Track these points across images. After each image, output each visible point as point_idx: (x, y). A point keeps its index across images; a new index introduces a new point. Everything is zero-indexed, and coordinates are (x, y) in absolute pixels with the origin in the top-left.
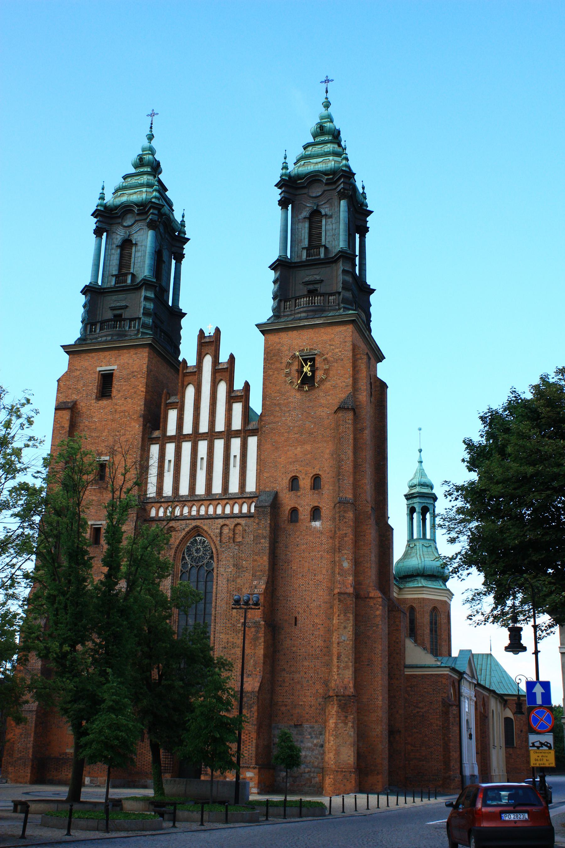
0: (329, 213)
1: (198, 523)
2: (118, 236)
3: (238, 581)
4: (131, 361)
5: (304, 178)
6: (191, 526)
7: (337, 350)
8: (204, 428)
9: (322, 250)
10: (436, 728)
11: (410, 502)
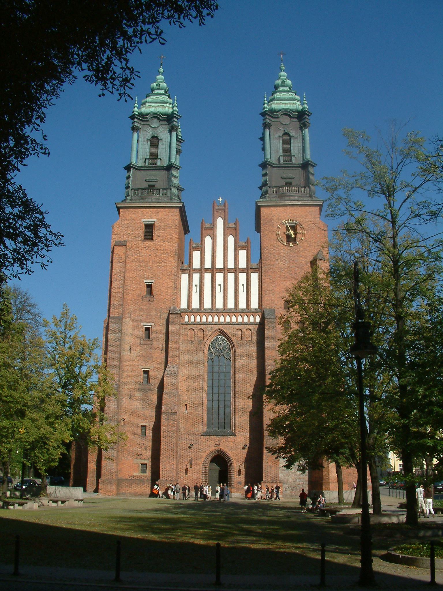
0: (296, 136)
1: (220, 327)
2: (148, 133)
3: (250, 365)
4: (166, 217)
5: (278, 112)
6: (214, 329)
7: (310, 223)
8: (219, 265)
9: (293, 158)
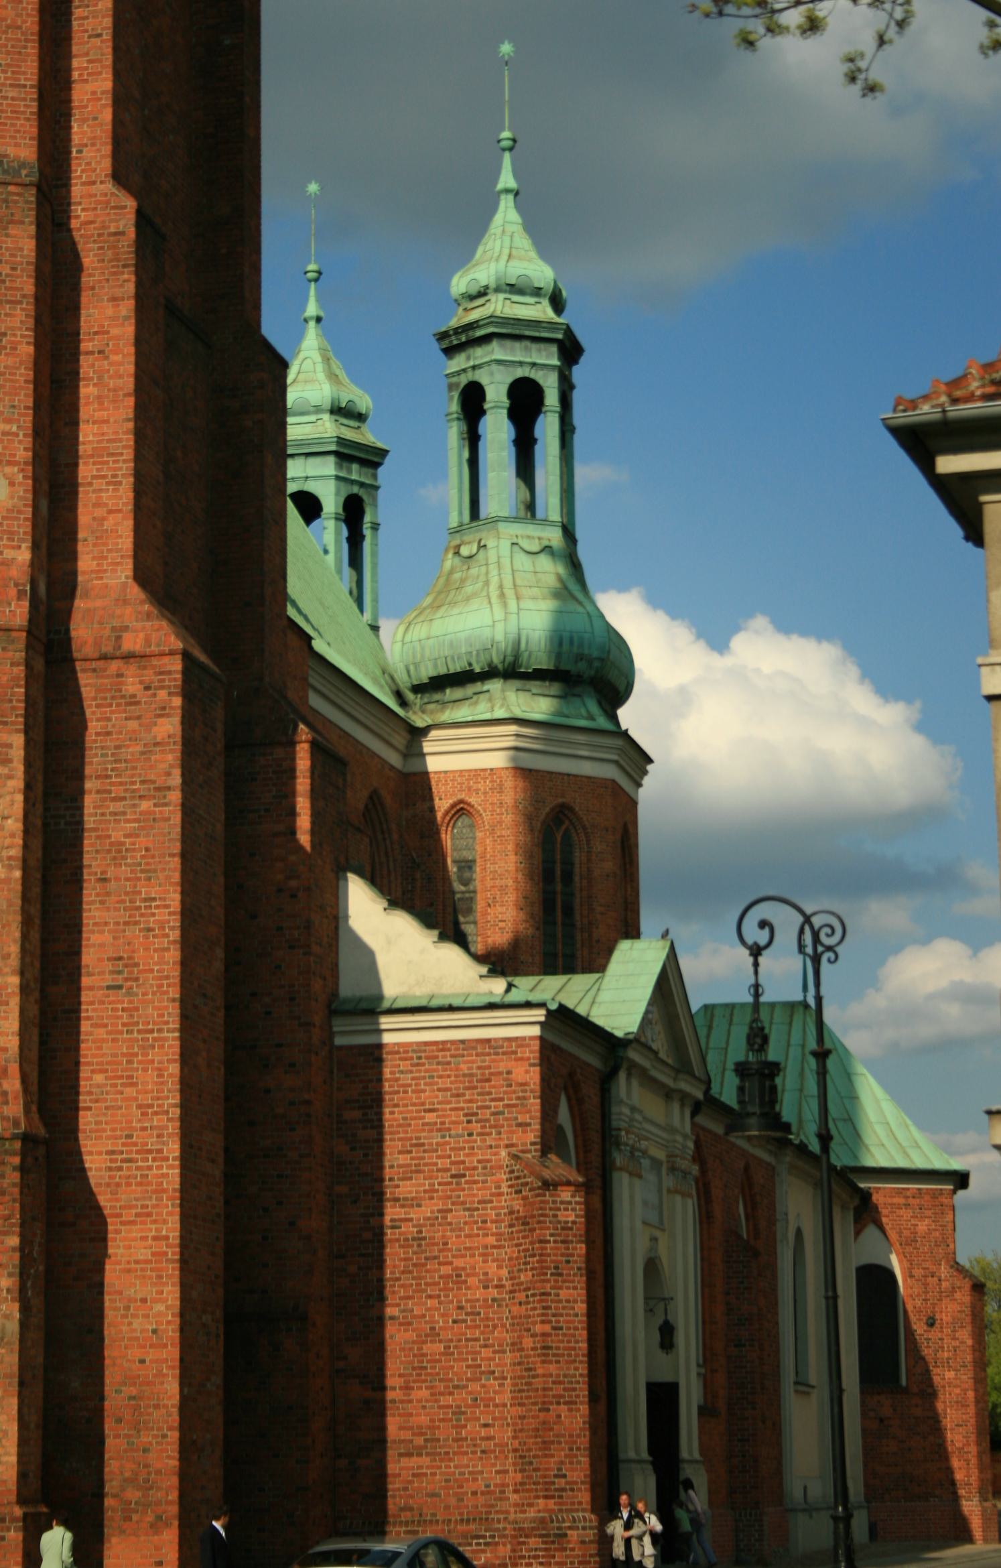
10: (479, 1294)
11: (459, 362)
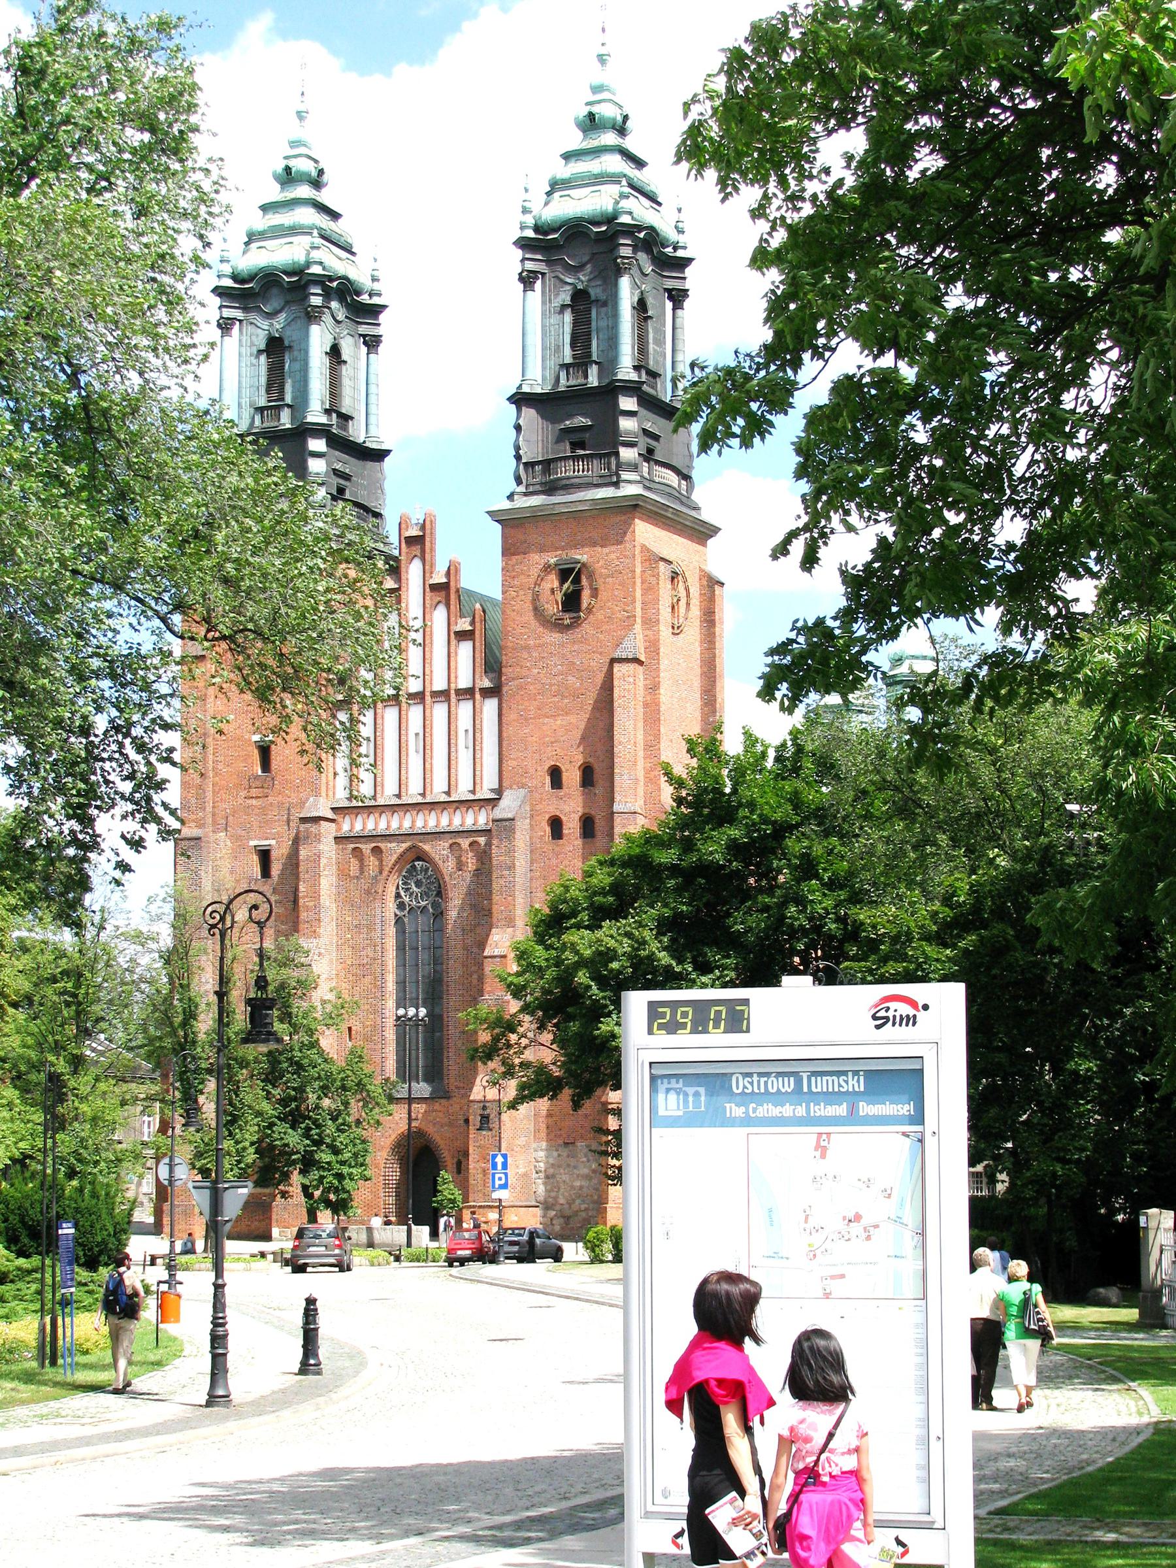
0: (603, 297)
7: (613, 556)
